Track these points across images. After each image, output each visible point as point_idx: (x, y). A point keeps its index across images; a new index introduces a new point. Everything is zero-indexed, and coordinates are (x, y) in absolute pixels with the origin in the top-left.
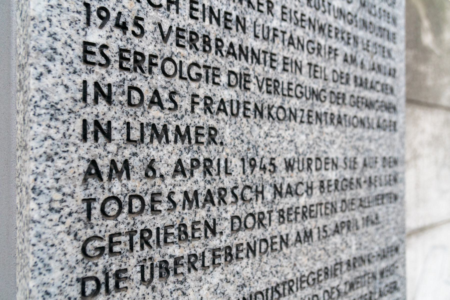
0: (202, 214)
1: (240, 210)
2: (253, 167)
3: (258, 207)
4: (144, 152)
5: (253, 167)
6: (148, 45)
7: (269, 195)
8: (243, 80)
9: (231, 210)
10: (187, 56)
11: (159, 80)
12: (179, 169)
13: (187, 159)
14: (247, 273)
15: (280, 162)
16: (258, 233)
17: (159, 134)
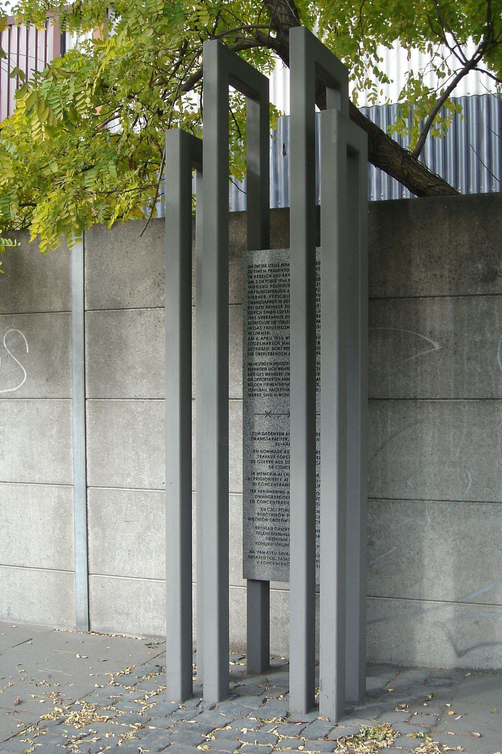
0: (266, 346)
1: (274, 346)
2: (277, 338)
3: (278, 346)
4: (256, 336)
5: (277, 338)
6: (257, 320)
7: (281, 344)
8: (275, 322)
9: (272, 346)
10: (263, 320)
11: (258, 325)
12: (262, 338)
13: (263, 337)
14: (276, 358)
15: (284, 338)
16: (279, 351)
17: (258, 333)
